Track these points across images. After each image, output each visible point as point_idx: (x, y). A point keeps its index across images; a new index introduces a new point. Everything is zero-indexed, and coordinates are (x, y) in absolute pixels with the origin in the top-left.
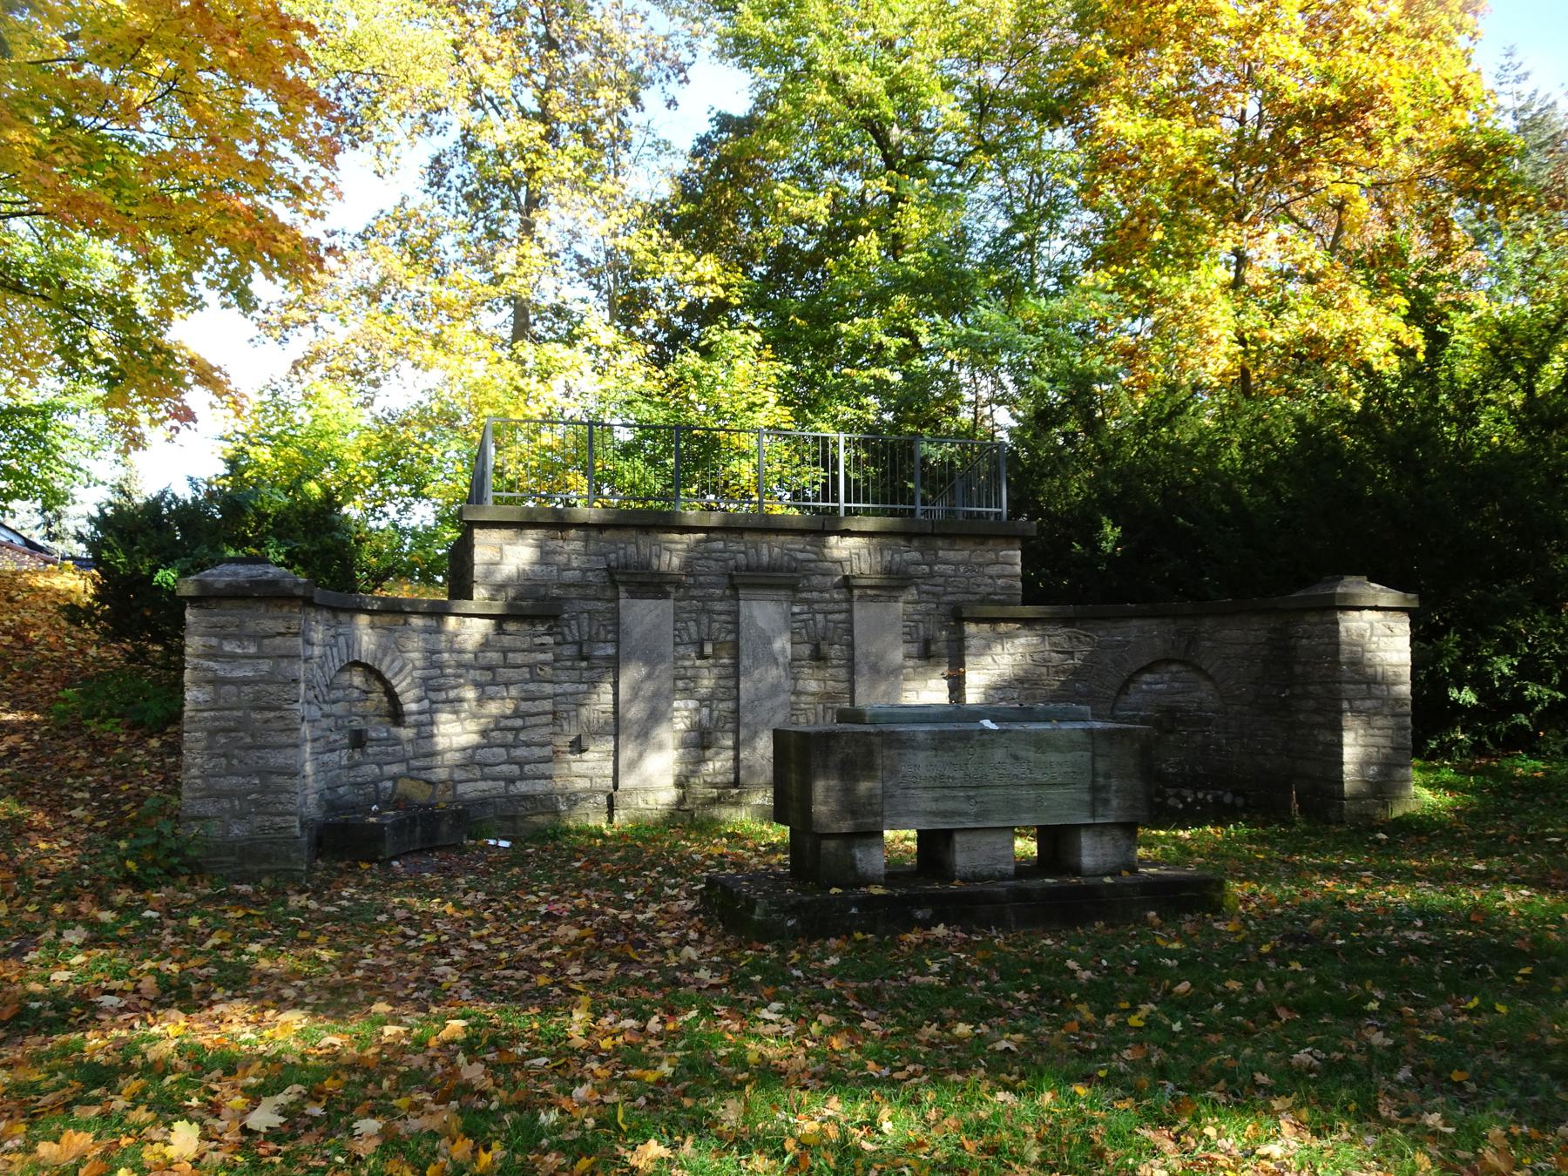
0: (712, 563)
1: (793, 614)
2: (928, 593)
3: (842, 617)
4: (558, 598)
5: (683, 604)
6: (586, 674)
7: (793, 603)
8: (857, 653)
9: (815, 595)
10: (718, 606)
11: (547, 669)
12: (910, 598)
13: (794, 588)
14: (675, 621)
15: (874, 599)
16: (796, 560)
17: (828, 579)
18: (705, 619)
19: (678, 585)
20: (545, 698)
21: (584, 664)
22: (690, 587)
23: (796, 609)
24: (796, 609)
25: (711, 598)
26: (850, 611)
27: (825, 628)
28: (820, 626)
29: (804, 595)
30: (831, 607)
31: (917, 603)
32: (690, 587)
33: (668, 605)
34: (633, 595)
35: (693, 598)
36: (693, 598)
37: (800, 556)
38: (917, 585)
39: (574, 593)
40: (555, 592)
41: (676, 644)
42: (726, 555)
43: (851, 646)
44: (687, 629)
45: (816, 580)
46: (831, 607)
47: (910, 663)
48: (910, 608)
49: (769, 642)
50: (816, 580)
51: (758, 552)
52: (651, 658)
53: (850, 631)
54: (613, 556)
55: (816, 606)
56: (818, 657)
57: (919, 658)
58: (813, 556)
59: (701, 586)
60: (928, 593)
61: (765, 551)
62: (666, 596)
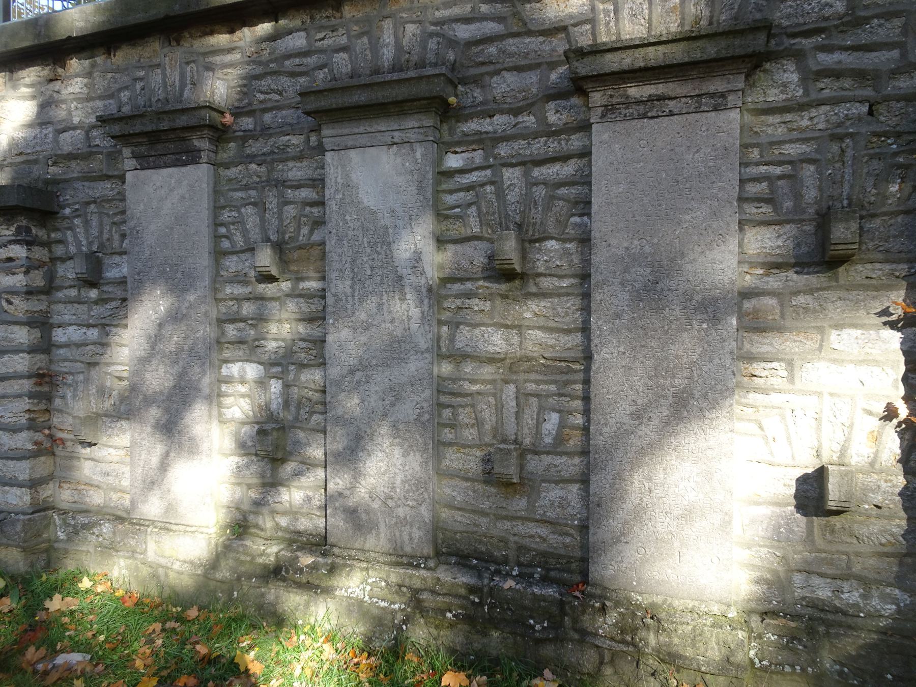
0: (285, 81)
1: (450, 174)
2: (836, 74)
3: (568, 169)
4: (55, 182)
5: (233, 172)
6: (97, 310)
7: (447, 147)
8: (599, 257)
9: (500, 122)
10: (296, 171)
11: (16, 301)
12: (774, 96)
13: (445, 112)
14: (217, 209)
15: (649, 109)
16: (452, 43)
17: (532, 78)
18: (272, 202)
19: (220, 134)
20: (16, 351)
21: (93, 294)
22: (248, 136)
23: (453, 161)
24: (453, 161)
25: (281, 156)
26: (585, 153)
27: (528, 200)
28: (512, 197)
29: (473, 126)
30: (538, 147)
31: (801, 107)
32: (248, 136)
33: (198, 176)
34: (145, 163)
35: (251, 158)
36: (251, 158)
37: (464, 32)
38: (798, 56)
39: (76, 169)
40: (54, 170)
41: (219, 254)
42: (312, 61)
43: (585, 240)
44: (240, 222)
45: (505, 85)
46: (538, 147)
47: (774, 282)
48: (773, 127)
49: (384, 241)
50: (505, 85)
51: (375, 46)
52: (177, 281)
53: (584, 206)
54: (125, 96)
55: (503, 150)
56: (507, 276)
58: (491, 27)
59: (265, 132)
60: (836, 74)
61: (388, 37)
62: (192, 157)
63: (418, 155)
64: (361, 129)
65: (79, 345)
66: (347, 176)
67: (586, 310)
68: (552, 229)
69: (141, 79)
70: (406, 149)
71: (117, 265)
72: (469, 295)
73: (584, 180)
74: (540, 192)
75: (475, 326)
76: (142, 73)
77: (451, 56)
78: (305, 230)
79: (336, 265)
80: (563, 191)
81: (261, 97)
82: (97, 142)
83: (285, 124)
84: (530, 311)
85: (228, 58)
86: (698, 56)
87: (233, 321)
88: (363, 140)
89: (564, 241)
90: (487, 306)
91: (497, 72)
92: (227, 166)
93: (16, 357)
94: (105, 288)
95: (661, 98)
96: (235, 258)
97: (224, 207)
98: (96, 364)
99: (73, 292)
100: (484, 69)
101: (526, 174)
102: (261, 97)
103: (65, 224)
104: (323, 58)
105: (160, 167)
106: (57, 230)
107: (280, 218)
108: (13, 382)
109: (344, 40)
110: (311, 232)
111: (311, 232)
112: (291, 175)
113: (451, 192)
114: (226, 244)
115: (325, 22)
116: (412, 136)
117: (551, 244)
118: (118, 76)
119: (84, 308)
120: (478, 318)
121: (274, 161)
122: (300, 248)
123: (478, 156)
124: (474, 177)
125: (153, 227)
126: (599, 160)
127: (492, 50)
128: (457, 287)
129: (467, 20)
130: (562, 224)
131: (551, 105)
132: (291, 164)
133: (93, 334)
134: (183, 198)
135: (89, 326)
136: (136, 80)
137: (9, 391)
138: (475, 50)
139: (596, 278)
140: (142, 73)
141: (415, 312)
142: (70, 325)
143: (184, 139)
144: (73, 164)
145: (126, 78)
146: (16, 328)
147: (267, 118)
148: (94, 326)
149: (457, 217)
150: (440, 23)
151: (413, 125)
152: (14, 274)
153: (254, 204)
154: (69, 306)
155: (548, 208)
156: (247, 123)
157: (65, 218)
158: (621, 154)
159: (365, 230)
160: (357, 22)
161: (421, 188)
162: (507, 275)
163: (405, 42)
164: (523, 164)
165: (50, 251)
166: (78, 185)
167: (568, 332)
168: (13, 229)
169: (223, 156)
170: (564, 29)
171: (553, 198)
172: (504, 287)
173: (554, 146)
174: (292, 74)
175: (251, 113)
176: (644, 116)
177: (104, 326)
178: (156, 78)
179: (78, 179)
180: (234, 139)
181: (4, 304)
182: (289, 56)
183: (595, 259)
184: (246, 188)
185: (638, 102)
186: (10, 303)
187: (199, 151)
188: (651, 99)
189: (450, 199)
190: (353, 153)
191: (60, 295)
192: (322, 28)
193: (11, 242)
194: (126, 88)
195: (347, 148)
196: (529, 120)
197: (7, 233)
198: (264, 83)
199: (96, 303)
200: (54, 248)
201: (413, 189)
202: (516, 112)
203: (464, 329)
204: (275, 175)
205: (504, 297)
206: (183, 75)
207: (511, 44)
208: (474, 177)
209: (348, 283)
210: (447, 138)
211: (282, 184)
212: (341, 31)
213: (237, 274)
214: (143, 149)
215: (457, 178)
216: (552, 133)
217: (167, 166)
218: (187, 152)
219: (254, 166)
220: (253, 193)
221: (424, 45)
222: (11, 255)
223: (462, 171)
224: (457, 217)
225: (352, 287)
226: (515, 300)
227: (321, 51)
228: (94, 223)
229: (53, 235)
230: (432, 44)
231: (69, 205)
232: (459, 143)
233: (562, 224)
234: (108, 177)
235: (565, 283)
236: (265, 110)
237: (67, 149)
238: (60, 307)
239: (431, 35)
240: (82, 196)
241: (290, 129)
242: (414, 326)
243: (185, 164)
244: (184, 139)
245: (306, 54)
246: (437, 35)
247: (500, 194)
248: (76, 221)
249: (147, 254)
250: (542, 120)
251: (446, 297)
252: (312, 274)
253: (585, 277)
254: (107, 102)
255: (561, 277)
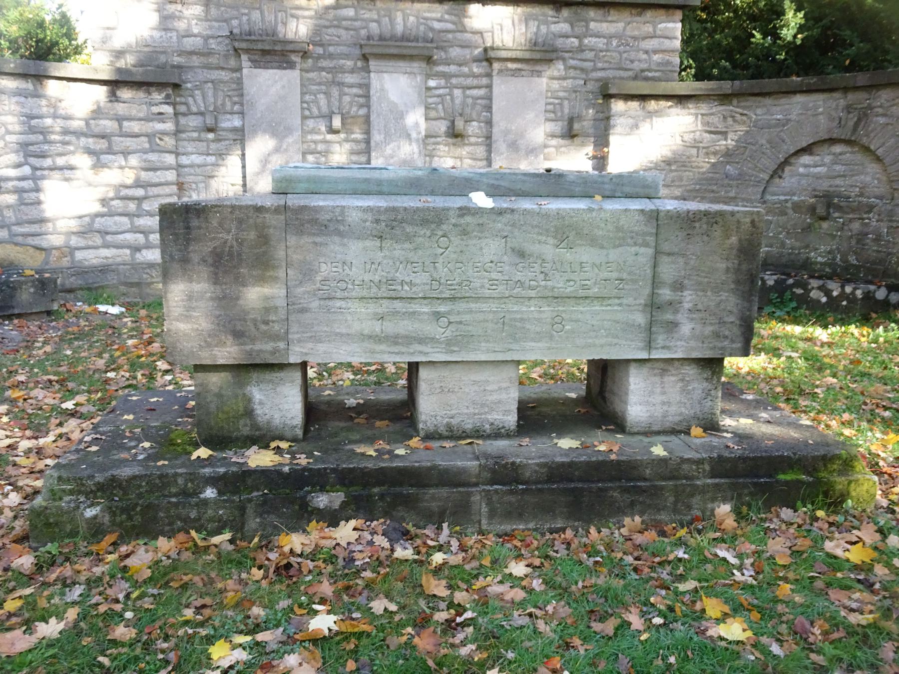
0: (342, 32)
1: (429, 89)
2: (575, 68)
3: (482, 92)
4: (179, 67)
5: (311, 75)
6: (213, 146)
7: (428, 76)
8: (495, 130)
9: (453, 68)
10: (350, 79)
11: (166, 139)
12: (556, 73)
13: (429, 60)
14: (303, 94)
15: (516, 73)
16: (432, 29)
17: (467, 51)
18: (335, 92)
19: (305, 55)
20: (167, 169)
21: (211, 136)
22: (319, 57)
23: (432, 83)
24: (432, 83)
25: (342, 70)
26: (489, 87)
27: (464, 104)
28: (457, 101)
29: (441, 68)
30: (469, 81)
31: (564, 79)
32: (319, 57)
33: (294, 75)
34: (256, 64)
35: (323, 69)
36: (323, 69)
37: (437, 25)
38: (564, 59)
39: (196, 61)
40: (177, 60)
41: (304, 118)
42: (358, 24)
43: (489, 123)
44: (316, 102)
45: (455, 52)
46: (469, 81)
47: (554, 142)
48: (555, 85)
49: (401, 116)
50: (455, 52)
51: (392, 21)
52: (278, 130)
53: (489, 108)
54: (235, 23)
55: (454, 81)
56: (455, 135)
57: (563, 137)
58: (450, 26)
59: (331, 56)
60: (575, 68)
61: (399, 19)
62: (291, 66)
63: (418, 79)
64: (391, 64)
65: (199, 166)
66: (382, 85)
67: (489, 151)
68: (474, 116)
69: (245, 14)
70: (412, 76)
71: (229, 120)
72: (438, 143)
73: (490, 98)
74: (470, 101)
75: (440, 157)
76: (246, 11)
77: (431, 35)
78: (354, 109)
79: (376, 128)
80: (479, 101)
81: (328, 38)
82: (213, 46)
83: (342, 54)
84: (464, 151)
85: (307, 13)
86: (534, 57)
87: (312, 153)
88: (391, 69)
89: (480, 122)
90: (447, 149)
91: (452, 46)
92: (307, 71)
93: (167, 172)
94: (221, 133)
95: (520, 70)
96: (312, 120)
97: (306, 93)
98: (212, 177)
99: (195, 135)
100: (445, 44)
101: (464, 93)
102: (328, 38)
103: (187, 93)
104: (364, 24)
105: (268, 68)
106: (181, 96)
107: (340, 101)
108: (165, 187)
109: (376, 17)
110: (358, 110)
111: (358, 110)
112: (346, 80)
113: (431, 97)
114: (307, 113)
115: (366, 6)
116: (415, 70)
117: (475, 123)
118: (229, 10)
119: (205, 144)
120: (442, 154)
121: (337, 72)
122: (352, 117)
123: (443, 82)
124: (441, 91)
125: (263, 101)
126: (496, 90)
127: (450, 36)
128: (433, 140)
129: (439, 21)
130: (479, 115)
131: (475, 64)
132: (346, 75)
133: (211, 159)
134: (284, 87)
135: (208, 154)
136: (243, 14)
137: (161, 192)
138: (442, 34)
139: (494, 138)
140: (246, 11)
141: (416, 150)
142: (193, 154)
143: (286, 56)
144: (195, 58)
145: (235, 12)
146: (167, 155)
147: (331, 49)
148: (211, 155)
149: (433, 109)
150: (426, 19)
151: (416, 65)
152: (164, 122)
153: (325, 93)
154: (192, 143)
155: (473, 109)
156: (320, 50)
157: (187, 89)
158: (504, 89)
159: (391, 111)
160: (383, 10)
161: (419, 94)
162: (456, 136)
163: (409, 24)
164: (463, 88)
165: (174, 109)
166: (199, 71)
167: (481, 160)
168: (163, 95)
169: (305, 66)
170: (481, 33)
171: (475, 104)
172: (454, 140)
173: (475, 82)
174: (347, 29)
175: (322, 45)
176: (513, 75)
177: (220, 155)
178: (256, 15)
179: (198, 67)
180: (312, 57)
181: (157, 140)
182: (345, 19)
183: (494, 131)
184: (320, 84)
185: (511, 70)
186: (161, 139)
187: (295, 63)
188: (516, 69)
189: (430, 100)
190: (385, 75)
191: (184, 136)
192: (363, 8)
193: (161, 103)
194: (237, 18)
195: (382, 72)
196: (465, 69)
197: (159, 97)
198: (330, 31)
199: (213, 141)
200: (178, 107)
201: (416, 95)
202: (460, 65)
203: (436, 159)
204: (337, 80)
205: (454, 144)
206: (276, 17)
207: (458, 35)
208: (441, 91)
209: (383, 136)
210: (429, 72)
211: (341, 84)
212: (374, 12)
213: (313, 129)
214: (256, 57)
215: (433, 91)
216: (475, 76)
217: (272, 68)
218: (287, 63)
219: (324, 73)
220: (324, 87)
221: (418, 27)
222: (162, 111)
223: (436, 88)
224: (433, 109)
225: (385, 138)
226: (459, 146)
227: (362, 20)
228: (210, 93)
229: (178, 99)
230: (422, 28)
231: (190, 82)
232: (435, 76)
233: (479, 115)
234: (223, 69)
235: (480, 140)
236: (330, 45)
237: (189, 48)
238: (185, 143)
239: (422, 24)
240: (201, 77)
241: (347, 56)
242: (416, 156)
243: (285, 68)
244: (286, 56)
245: (351, 19)
246: (425, 24)
247: (452, 99)
248: (196, 92)
249: (259, 115)
250: (471, 70)
251: (428, 144)
252: (358, 131)
253: (489, 137)
254: (221, 24)
255: (478, 137)
